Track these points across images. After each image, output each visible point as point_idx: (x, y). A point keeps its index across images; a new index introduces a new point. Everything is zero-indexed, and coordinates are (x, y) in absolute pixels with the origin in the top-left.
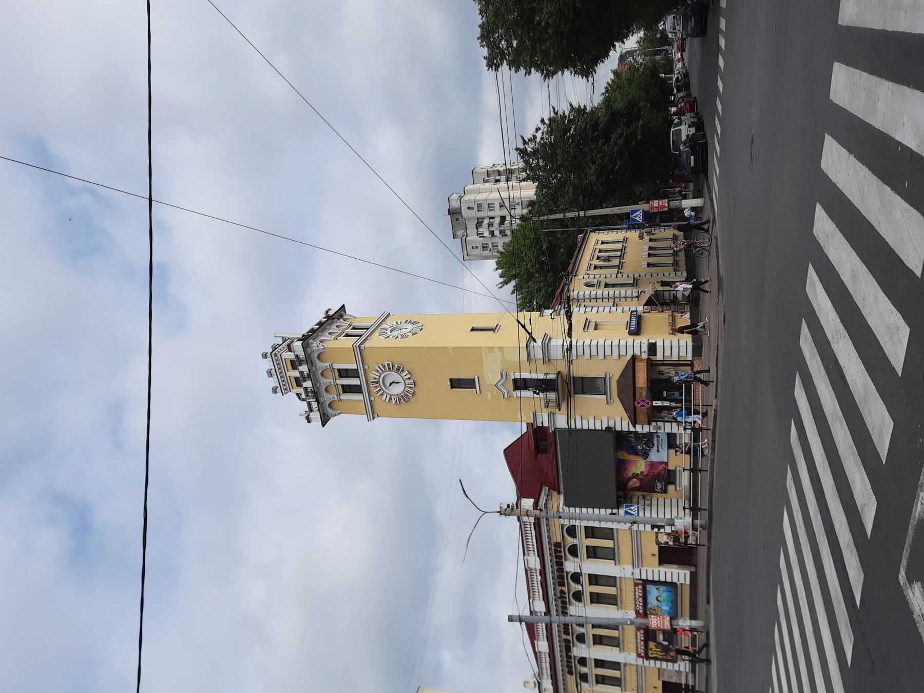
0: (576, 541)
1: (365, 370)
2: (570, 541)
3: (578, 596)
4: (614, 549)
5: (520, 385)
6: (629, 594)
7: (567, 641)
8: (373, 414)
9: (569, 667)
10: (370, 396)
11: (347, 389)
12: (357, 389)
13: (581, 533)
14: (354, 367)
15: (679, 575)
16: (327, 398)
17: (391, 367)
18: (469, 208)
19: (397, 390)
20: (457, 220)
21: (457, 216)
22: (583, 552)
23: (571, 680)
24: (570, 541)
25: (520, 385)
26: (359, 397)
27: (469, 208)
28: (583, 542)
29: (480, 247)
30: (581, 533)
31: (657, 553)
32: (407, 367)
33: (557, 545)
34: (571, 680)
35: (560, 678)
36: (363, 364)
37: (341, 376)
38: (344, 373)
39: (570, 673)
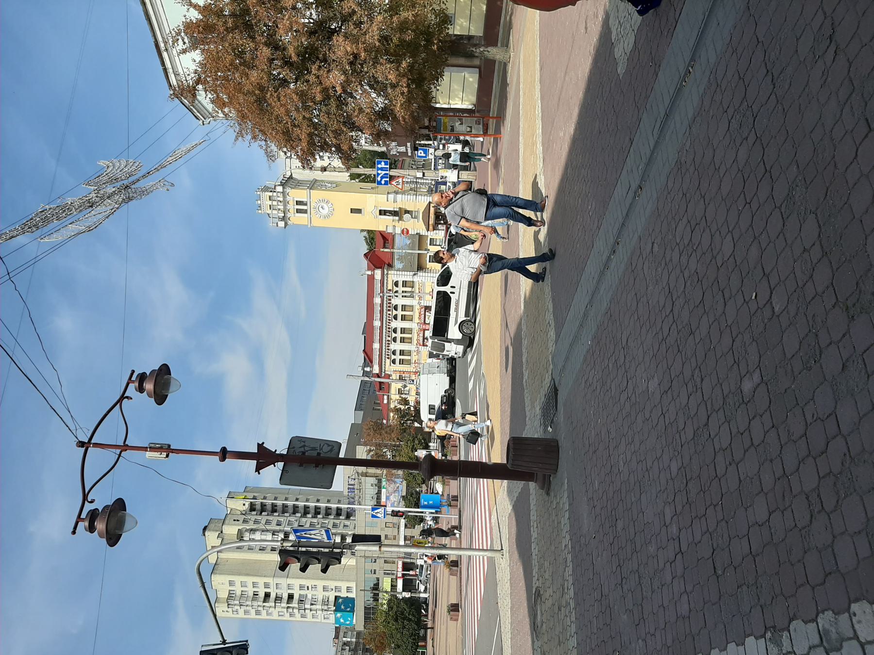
2: (395, 289)
3: (395, 317)
5: (383, 213)
11: (298, 211)
12: (305, 212)
14: (305, 200)
16: (289, 215)
17: (323, 201)
19: (325, 212)
23: (388, 361)
25: (383, 213)
26: (305, 215)
28: (401, 289)
30: (400, 284)
32: (331, 202)
34: (388, 361)
38: (298, 203)
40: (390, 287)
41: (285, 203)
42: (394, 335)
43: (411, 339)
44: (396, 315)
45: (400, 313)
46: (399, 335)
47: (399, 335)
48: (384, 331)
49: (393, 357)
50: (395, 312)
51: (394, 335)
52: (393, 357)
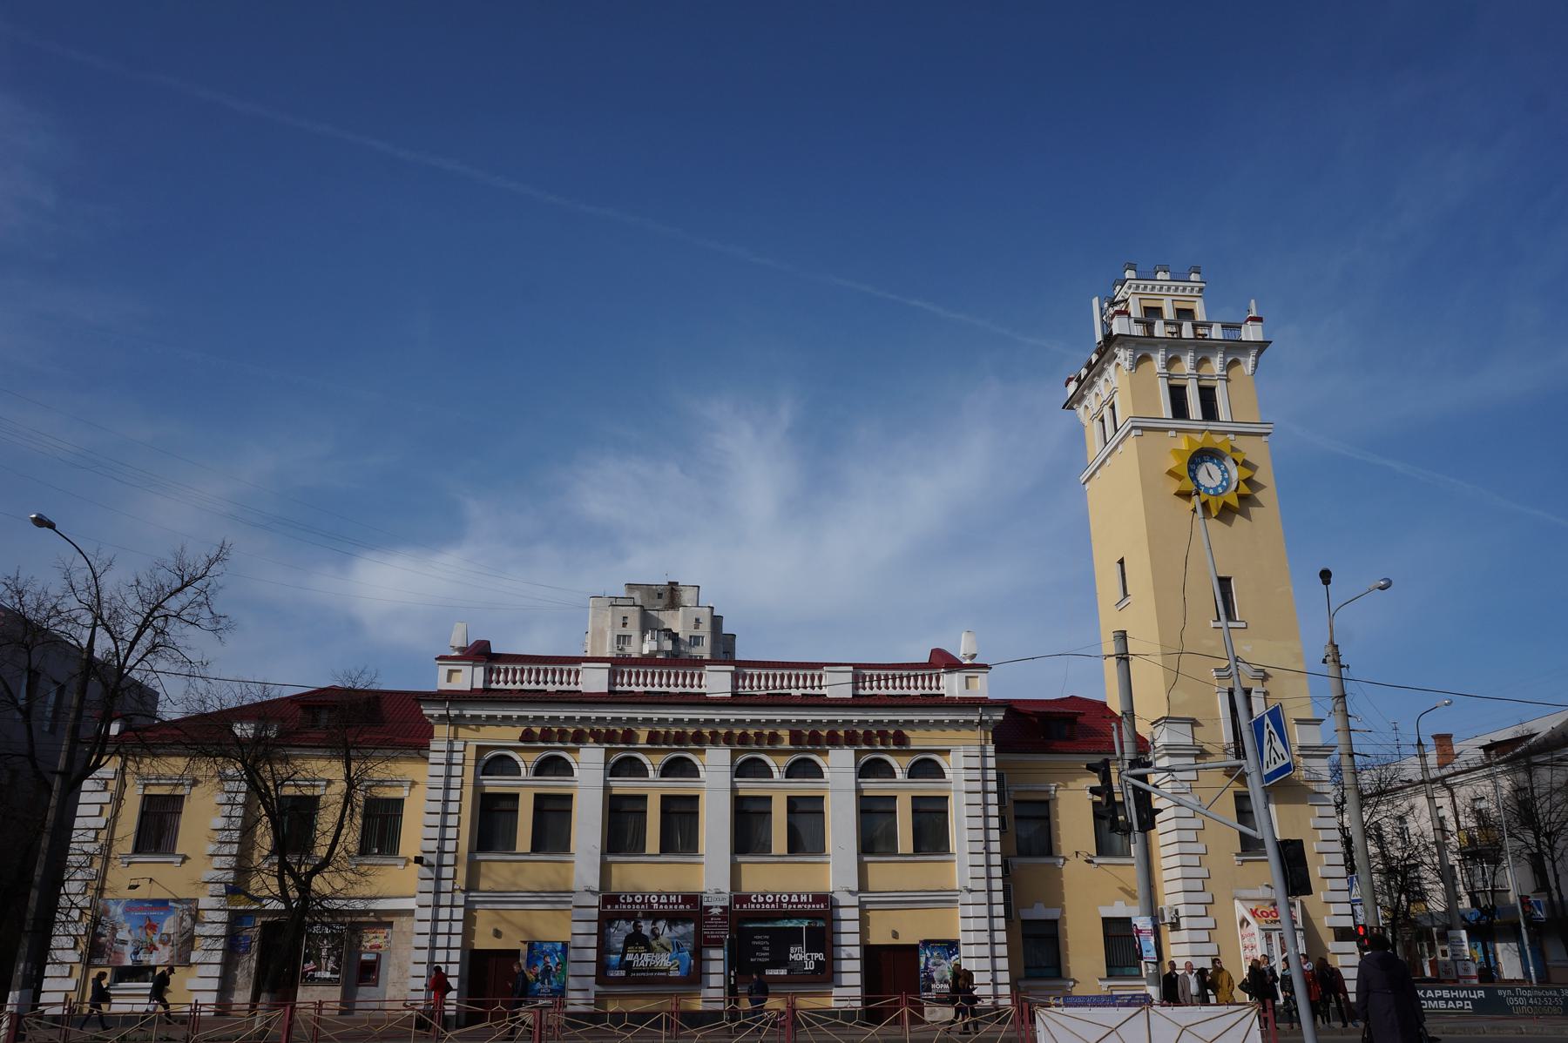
0: (900, 776)
1: (1225, 433)
2: (899, 764)
4: (895, 853)
6: (776, 878)
7: (629, 737)
8: (1143, 429)
9: (546, 736)
10: (1177, 430)
12: (1180, 410)
13: (926, 787)
14: (1223, 414)
15: (848, 990)
18: (697, 620)
20: (660, 596)
21: (666, 595)
22: (874, 787)
24: (899, 764)
27: (697, 620)
29: (624, 632)
30: (926, 787)
31: (902, 941)
33: (901, 739)
35: (515, 713)
36: (1236, 433)
37: (1201, 389)
38: (1207, 395)
39: (527, 736)
40: (918, 739)
41: (1203, 348)
42: (653, 763)
43: (638, 846)
44: (768, 773)
45: (778, 789)
46: (654, 787)
47: (654, 787)
48: (686, 714)
49: (526, 761)
50: (777, 765)
51: (653, 763)
52: (526, 761)
